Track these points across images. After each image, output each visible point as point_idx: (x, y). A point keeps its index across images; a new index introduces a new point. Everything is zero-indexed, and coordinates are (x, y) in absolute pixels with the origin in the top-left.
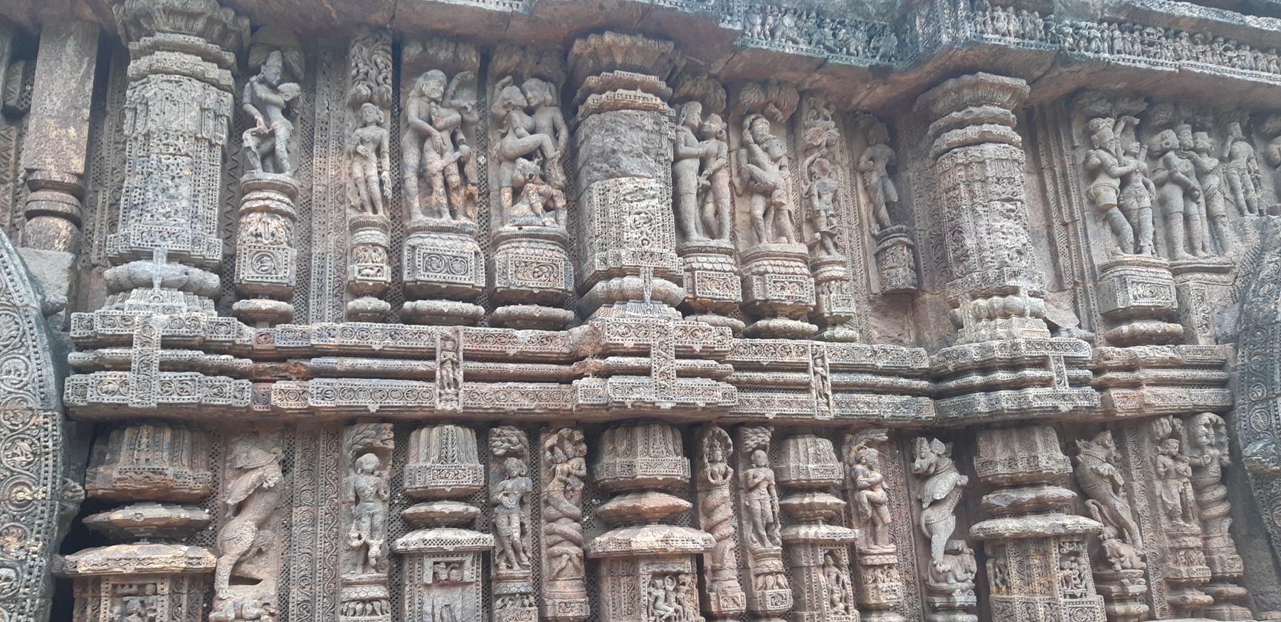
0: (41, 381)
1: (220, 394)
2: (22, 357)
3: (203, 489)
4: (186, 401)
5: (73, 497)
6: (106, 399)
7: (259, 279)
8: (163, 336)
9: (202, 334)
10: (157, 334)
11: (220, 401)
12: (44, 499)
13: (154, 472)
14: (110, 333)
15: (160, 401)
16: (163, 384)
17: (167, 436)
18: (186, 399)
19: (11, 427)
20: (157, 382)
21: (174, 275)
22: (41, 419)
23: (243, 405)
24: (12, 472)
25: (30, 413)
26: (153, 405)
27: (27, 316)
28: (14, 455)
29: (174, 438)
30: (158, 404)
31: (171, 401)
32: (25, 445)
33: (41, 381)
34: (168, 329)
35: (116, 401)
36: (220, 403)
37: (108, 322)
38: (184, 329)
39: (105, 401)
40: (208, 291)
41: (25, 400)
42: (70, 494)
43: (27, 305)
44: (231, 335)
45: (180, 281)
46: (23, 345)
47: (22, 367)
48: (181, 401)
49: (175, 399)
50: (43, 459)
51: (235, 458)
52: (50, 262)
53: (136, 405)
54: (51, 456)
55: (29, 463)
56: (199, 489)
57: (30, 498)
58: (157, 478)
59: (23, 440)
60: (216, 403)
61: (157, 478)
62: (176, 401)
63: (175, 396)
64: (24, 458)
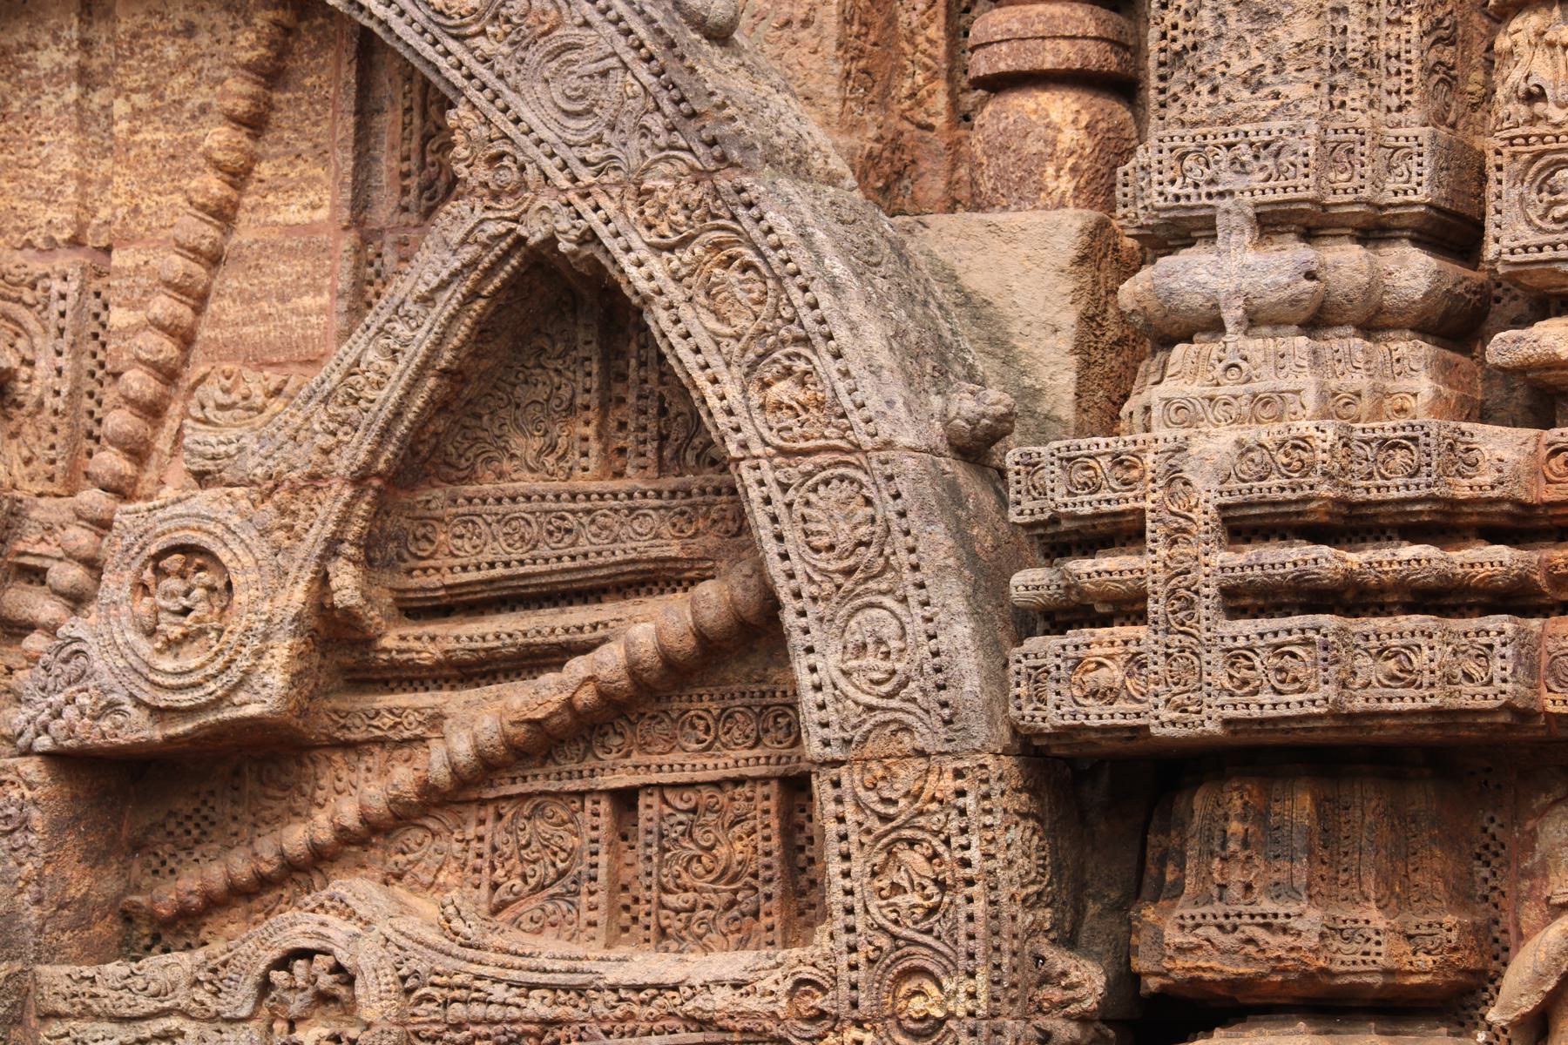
0: (938, 670)
1: (1405, 678)
2: (888, 601)
3: (1440, 968)
4: (1295, 711)
5: (1064, 1004)
6: (1096, 714)
7: (1548, 253)
8: (1222, 508)
9: (1325, 490)
10: (1206, 494)
11: (1407, 701)
12: (971, 1014)
13: (1267, 926)
14: (1087, 510)
15: (1230, 713)
16: (1233, 657)
17: (1299, 807)
18: (1293, 704)
19: (880, 808)
20: (1216, 656)
21: (1278, 286)
22: (949, 783)
23: (1490, 704)
24: (895, 937)
25: (921, 764)
26: (1210, 727)
27: (890, 478)
28: (896, 888)
29: (1318, 804)
30: (1227, 722)
31: (1255, 712)
32: (915, 859)
33: (938, 670)
34: (1233, 484)
35: (1119, 721)
36: (1408, 705)
37: (1080, 476)
38: (1274, 481)
39: (1094, 722)
40: (1401, 312)
41: (907, 729)
42: (1056, 994)
43: (888, 444)
44: (1422, 479)
45: (1295, 302)
46: (887, 566)
47: (890, 630)
48: (1282, 711)
49: (1265, 705)
50: (960, 900)
51: (1544, 865)
52: (1024, 250)
53: (1169, 731)
54: (976, 890)
55: (931, 911)
56: (1422, 967)
57: (939, 1013)
58: (1276, 944)
59: (912, 843)
60: (1396, 706)
61: (1276, 944)
62: (1269, 712)
63: (1266, 697)
64: (916, 898)
